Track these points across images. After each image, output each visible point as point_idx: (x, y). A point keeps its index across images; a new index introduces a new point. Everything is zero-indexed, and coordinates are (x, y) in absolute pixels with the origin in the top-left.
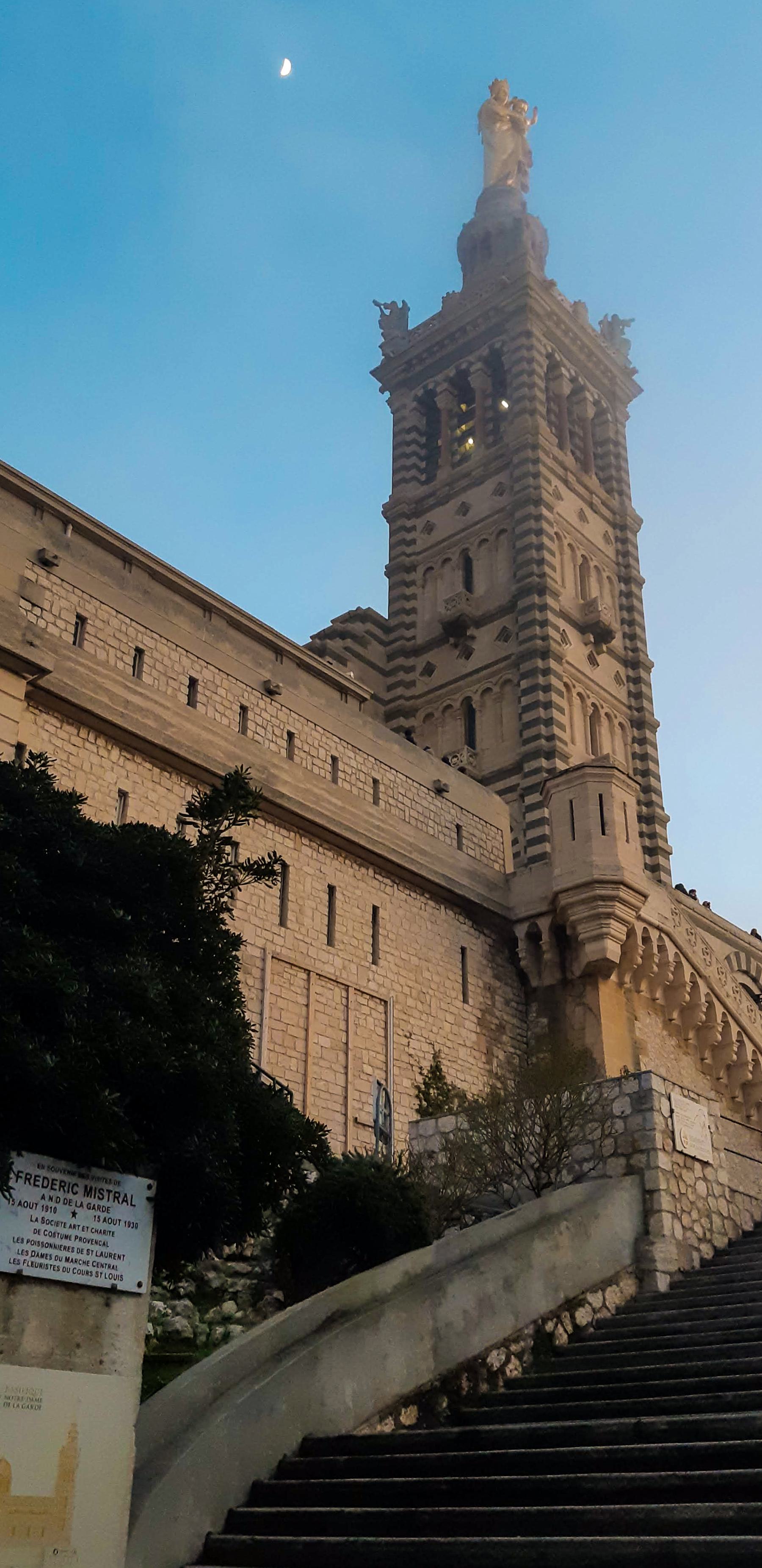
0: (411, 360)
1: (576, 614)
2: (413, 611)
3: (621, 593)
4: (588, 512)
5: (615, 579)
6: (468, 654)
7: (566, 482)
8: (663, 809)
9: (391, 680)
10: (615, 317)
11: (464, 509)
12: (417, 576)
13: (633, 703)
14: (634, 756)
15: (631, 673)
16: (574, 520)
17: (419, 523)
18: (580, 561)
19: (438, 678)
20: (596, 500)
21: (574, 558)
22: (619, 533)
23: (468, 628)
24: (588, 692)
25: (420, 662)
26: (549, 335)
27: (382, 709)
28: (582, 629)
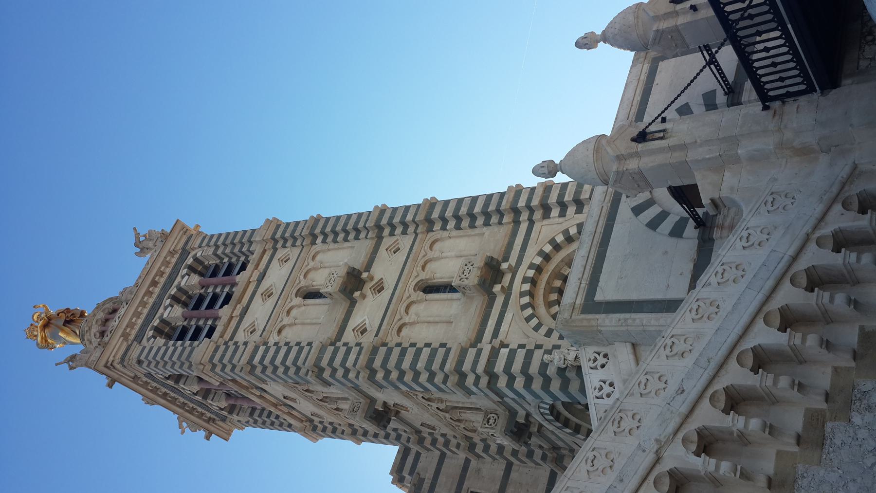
0: (204, 420)
1: (339, 313)
3: (324, 242)
8: (502, 194)
10: (136, 245)
13: (411, 229)
14: (458, 227)
15: (387, 231)
16: (271, 302)
18: (299, 300)
20: (256, 274)
21: (299, 306)
22: (279, 245)
23: (376, 410)
24: (404, 298)
26: (139, 338)
27: (474, 463)
28: (353, 303)
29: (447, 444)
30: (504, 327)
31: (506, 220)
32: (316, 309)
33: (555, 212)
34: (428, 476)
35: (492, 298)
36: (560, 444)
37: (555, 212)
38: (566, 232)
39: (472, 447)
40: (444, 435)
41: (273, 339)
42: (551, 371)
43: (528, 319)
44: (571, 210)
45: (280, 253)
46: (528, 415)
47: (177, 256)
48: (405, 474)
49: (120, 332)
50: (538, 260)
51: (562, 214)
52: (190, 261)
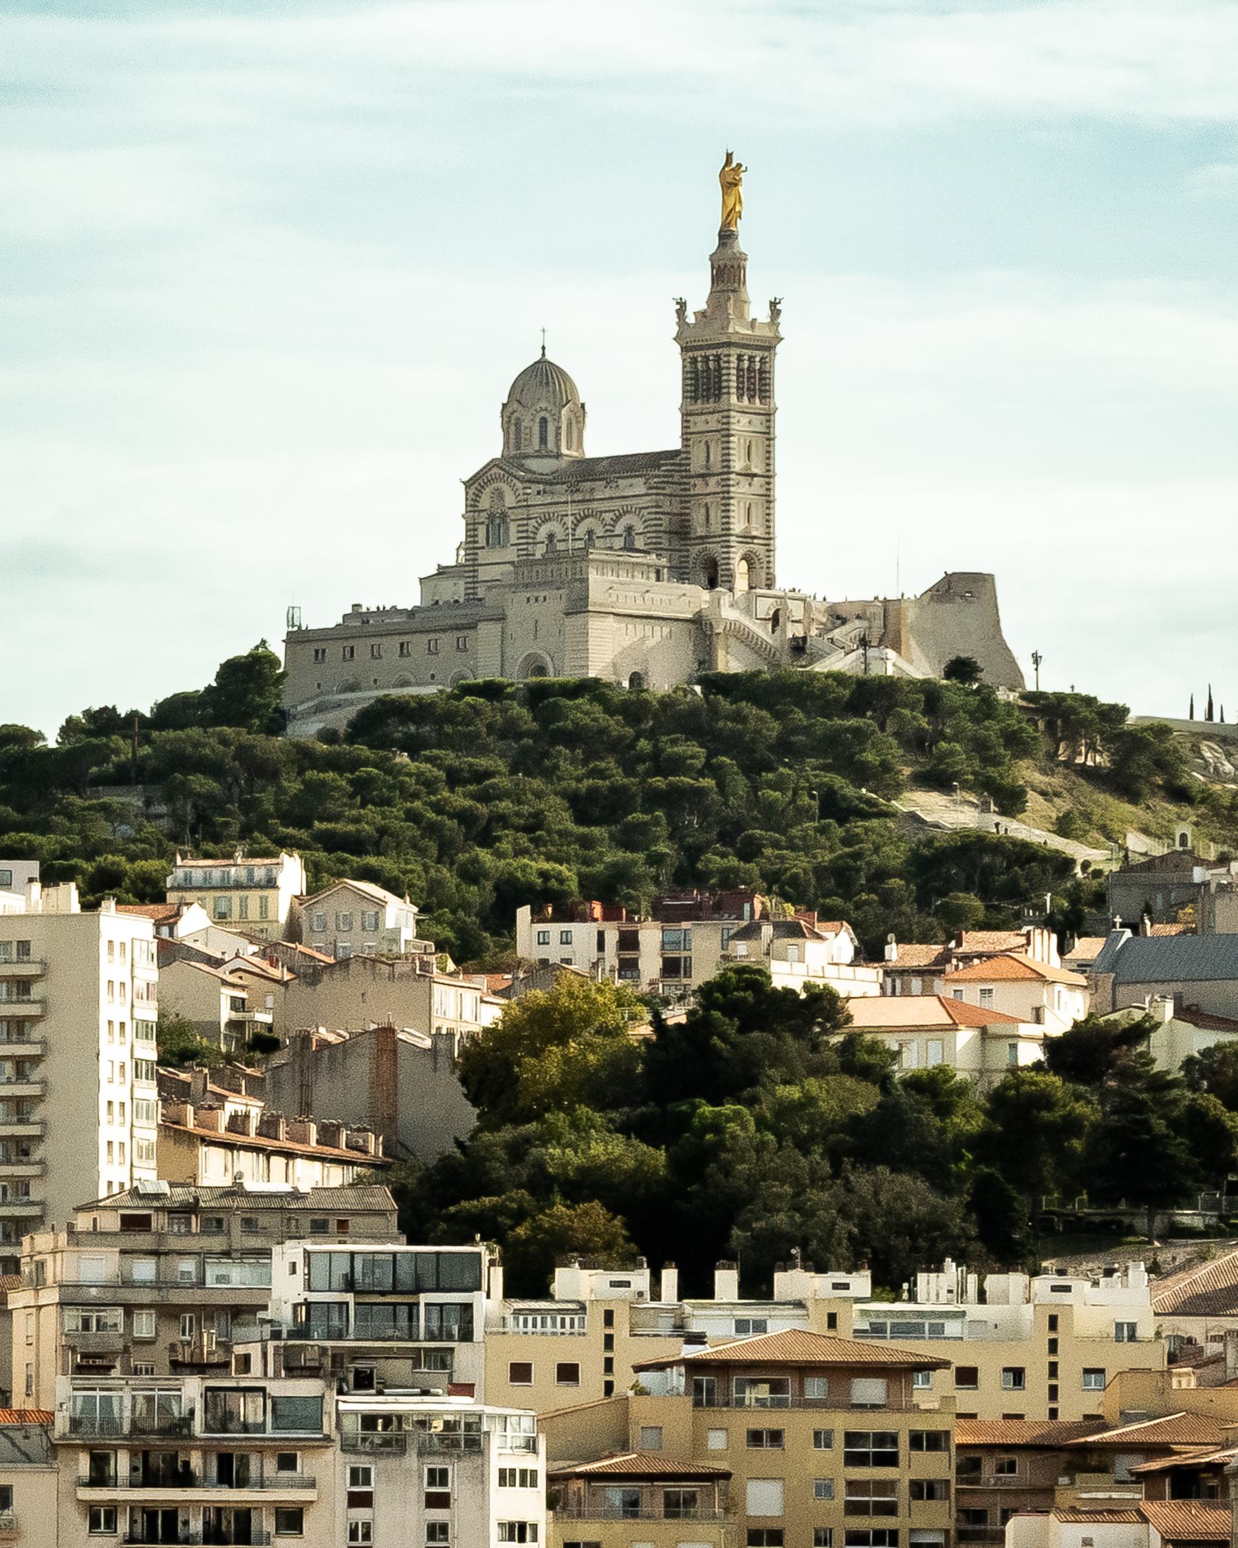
12: (691, 443)
25: (692, 481)
34: (676, 479)
35: (745, 537)
40: (689, 490)
46: (709, 543)
52: (766, 354)
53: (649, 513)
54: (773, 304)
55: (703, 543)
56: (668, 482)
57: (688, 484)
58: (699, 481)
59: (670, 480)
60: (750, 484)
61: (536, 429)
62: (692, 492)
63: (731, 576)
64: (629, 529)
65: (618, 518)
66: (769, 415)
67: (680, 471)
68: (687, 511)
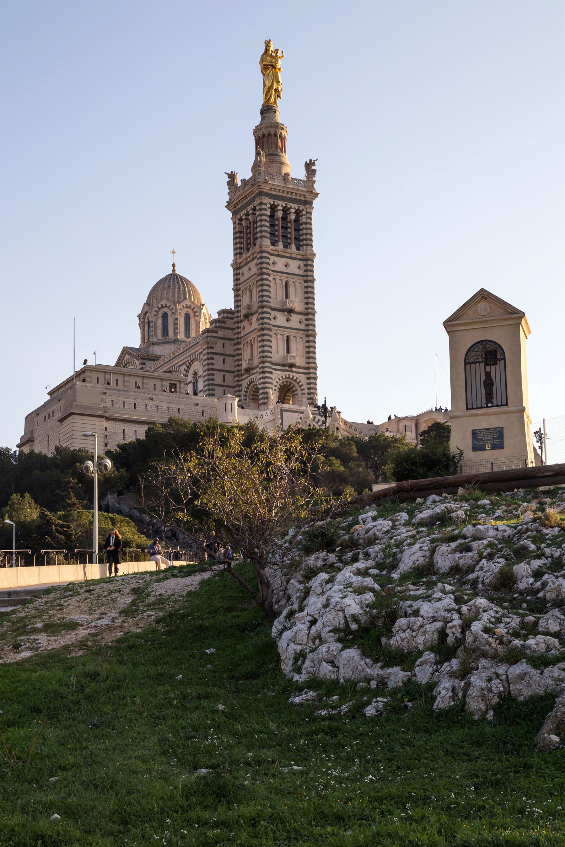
1: (280, 307)
2: (240, 306)
4: (290, 261)
5: (302, 282)
6: (251, 324)
7: (278, 256)
9: (235, 332)
10: (311, 160)
11: (250, 269)
12: (240, 293)
15: (307, 317)
17: (240, 271)
18: (284, 284)
19: (246, 331)
27: (233, 342)
28: (282, 311)
29: (238, 333)
30: (277, 372)
31: (307, 365)
32: (281, 292)
33: (308, 381)
35: (284, 365)
36: (244, 377)
37: (308, 381)
38: (302, 385)
39: (238, 344)
41: (271, 278)
42: (267, 390)
43: (279, 379)
44: (308, 386)
45: (302, 263)
46: (253, 374)
47: (304, 199)
48: (225, 315)
49: (272, 187)
50: (295, 378)
51: (309, 384)
53: (204, 356)
54: (309, 167)
55: (250, 376)
56: (219, 327)
57: (238, 328)
58: (245, 323)
59: (223, 325)
60: (287, 320)
61: (160, 322)
62: (242, 335)
63: (267, 398)
64: (195, 374)
65: (189, 367)
66: (306, 260)
67: (233, 318)
68: (240, 352)
